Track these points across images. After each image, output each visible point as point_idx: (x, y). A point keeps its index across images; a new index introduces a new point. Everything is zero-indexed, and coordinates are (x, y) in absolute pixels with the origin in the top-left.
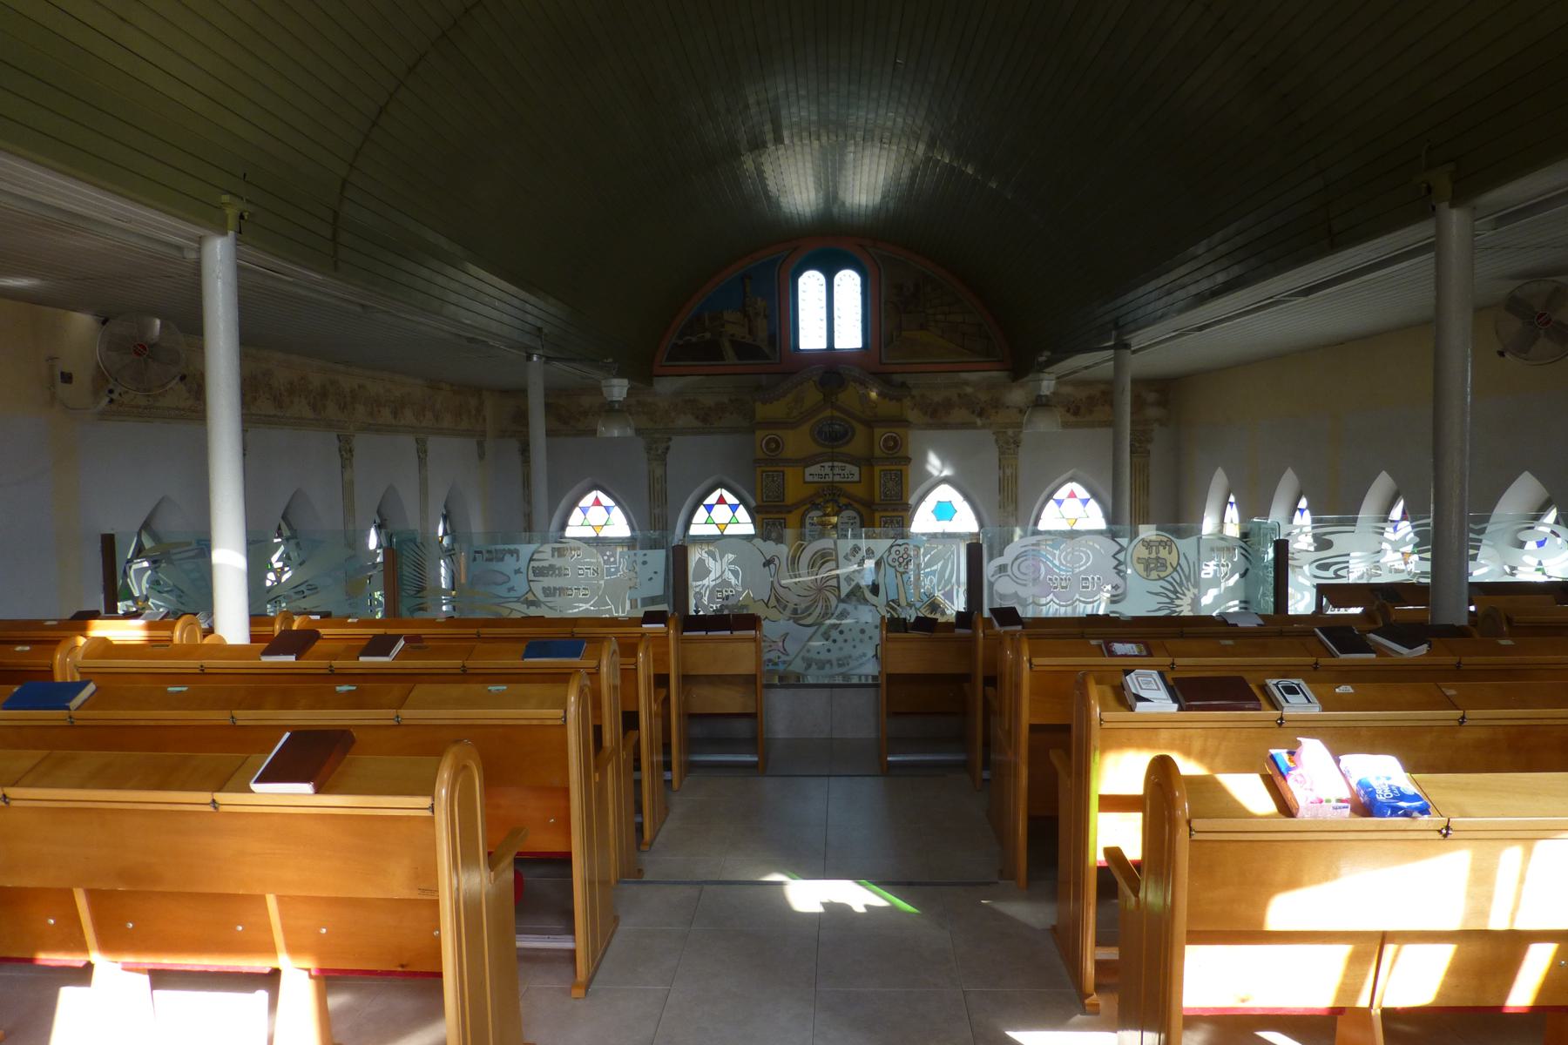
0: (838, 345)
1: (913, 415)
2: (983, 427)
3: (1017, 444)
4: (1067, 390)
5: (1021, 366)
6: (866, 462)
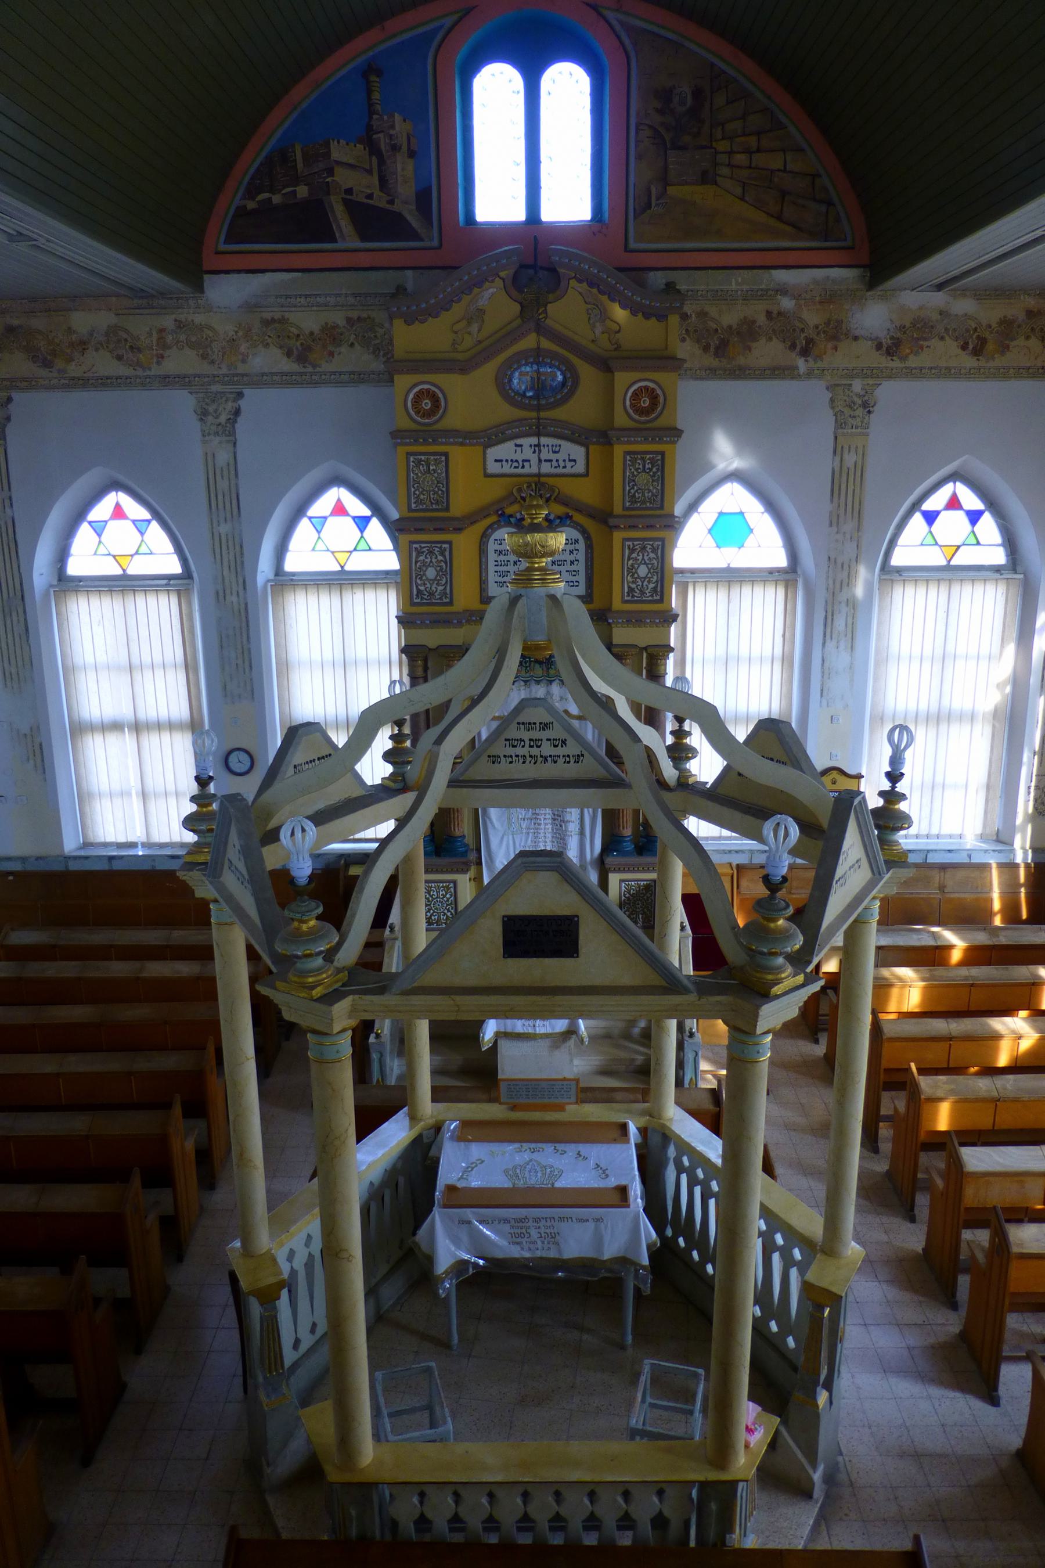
0: (549, 214)
1: (686, 350)
2: (810, 374)
3: (868, 407)
4: (964, 306)
5: (882, 261)
6: (599, 437)
